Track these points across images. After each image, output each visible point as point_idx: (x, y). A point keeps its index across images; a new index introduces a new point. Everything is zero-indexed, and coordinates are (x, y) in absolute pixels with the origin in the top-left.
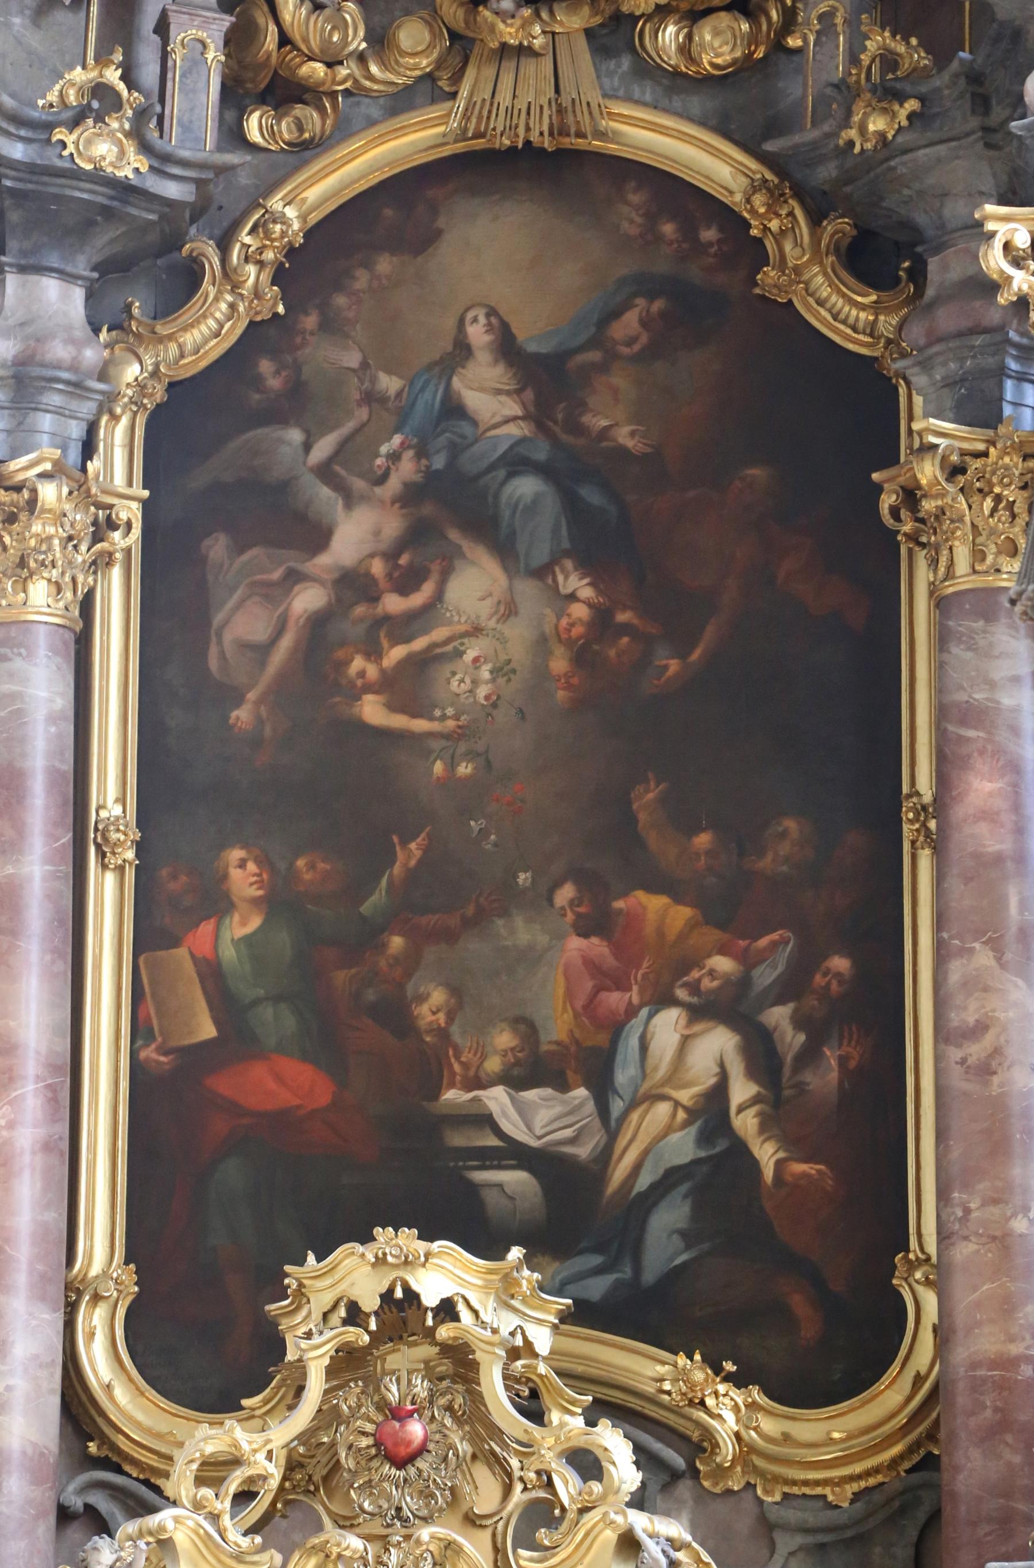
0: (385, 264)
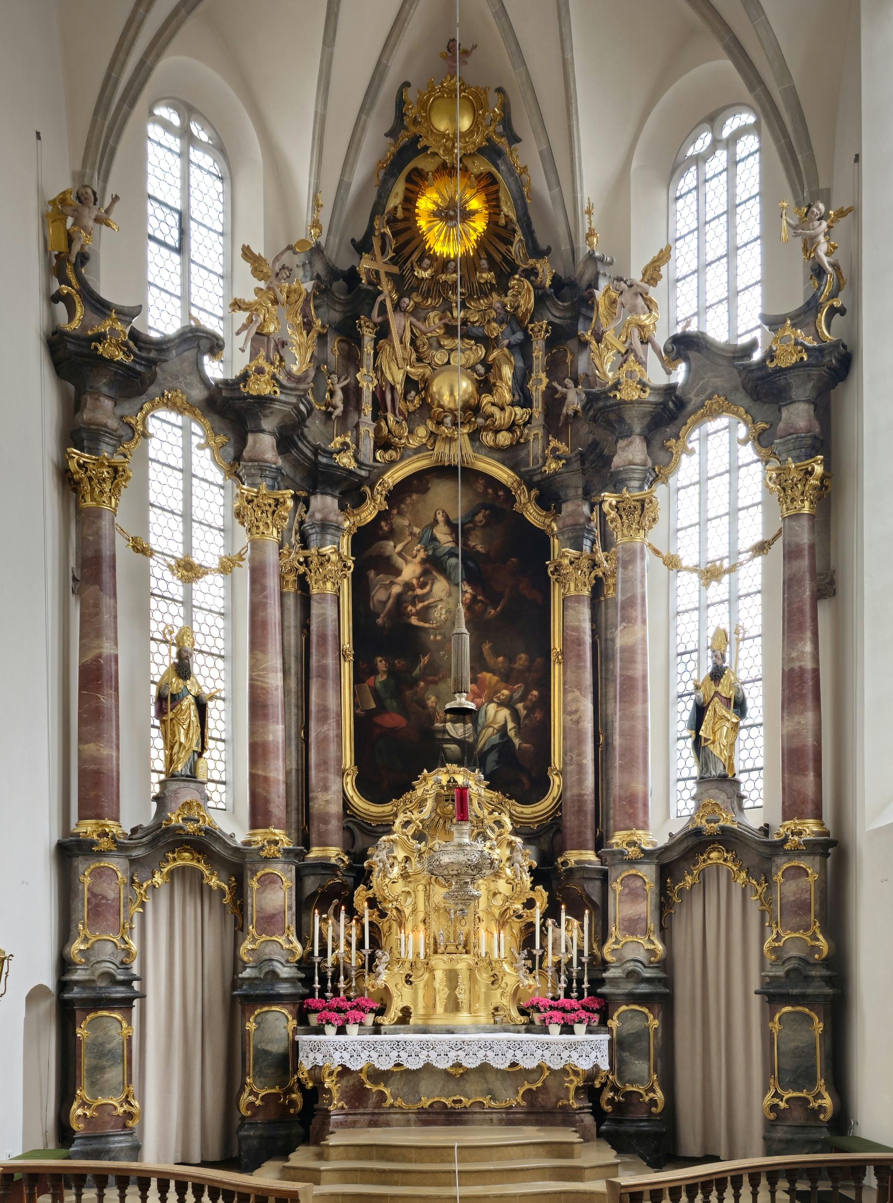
0: (415, 497)
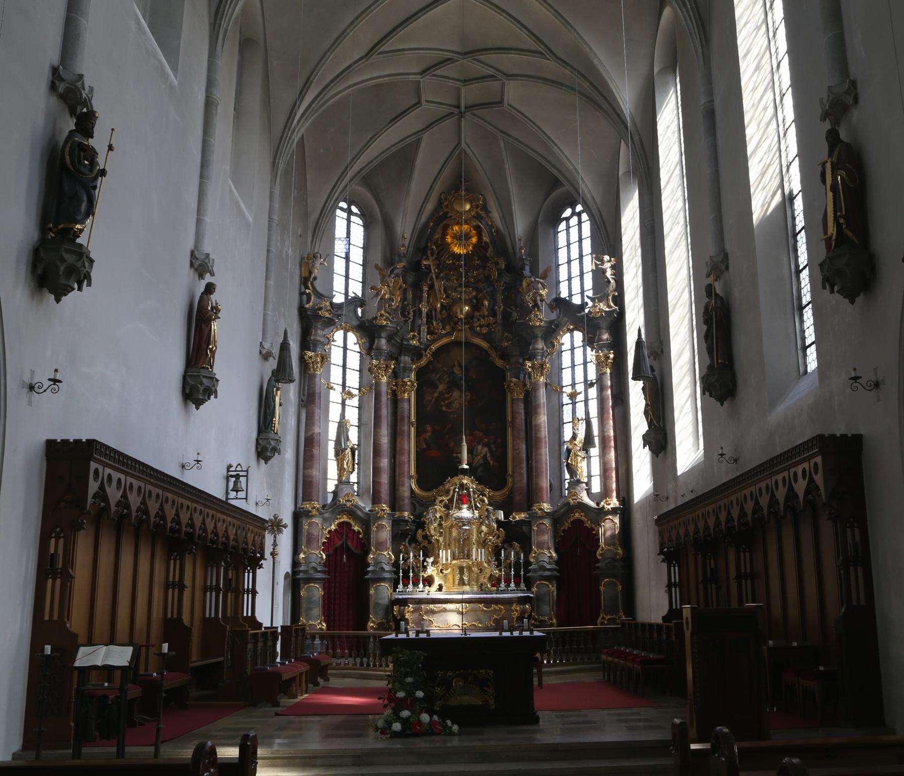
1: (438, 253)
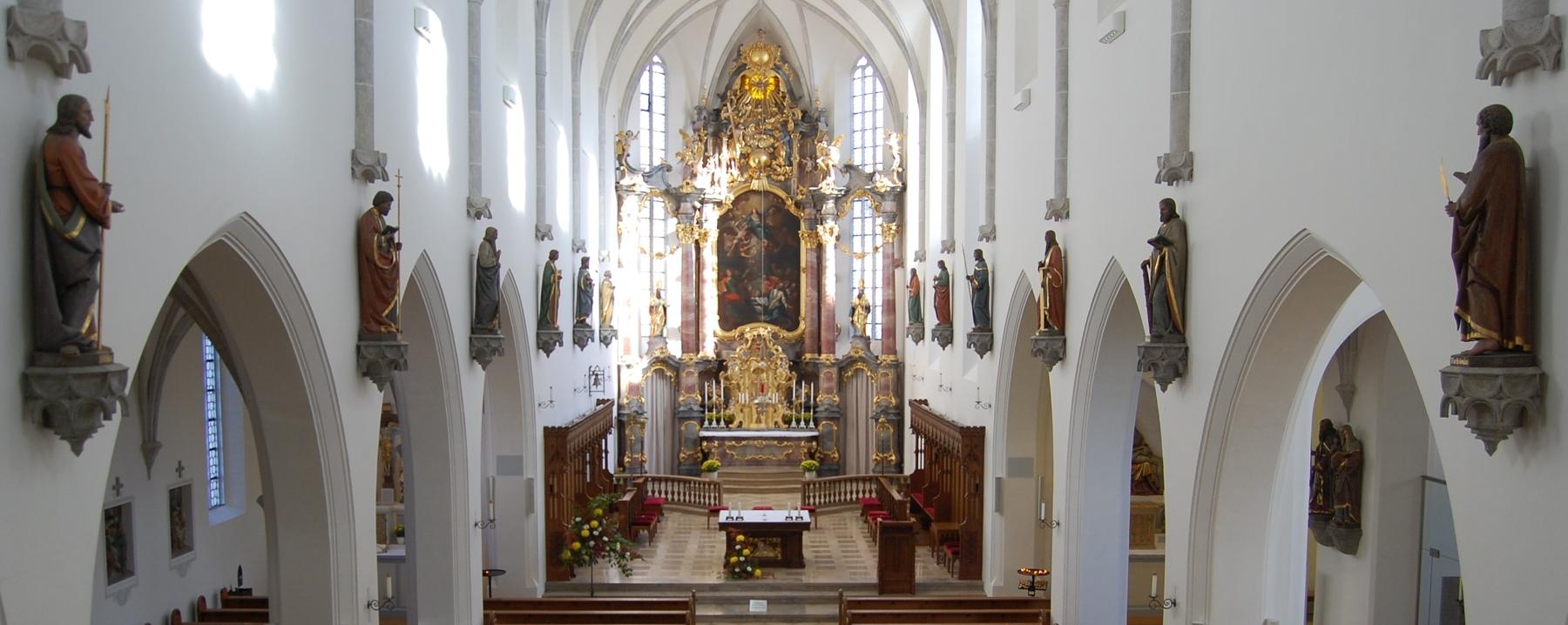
0: (744, 202)
1: (738, 100)
